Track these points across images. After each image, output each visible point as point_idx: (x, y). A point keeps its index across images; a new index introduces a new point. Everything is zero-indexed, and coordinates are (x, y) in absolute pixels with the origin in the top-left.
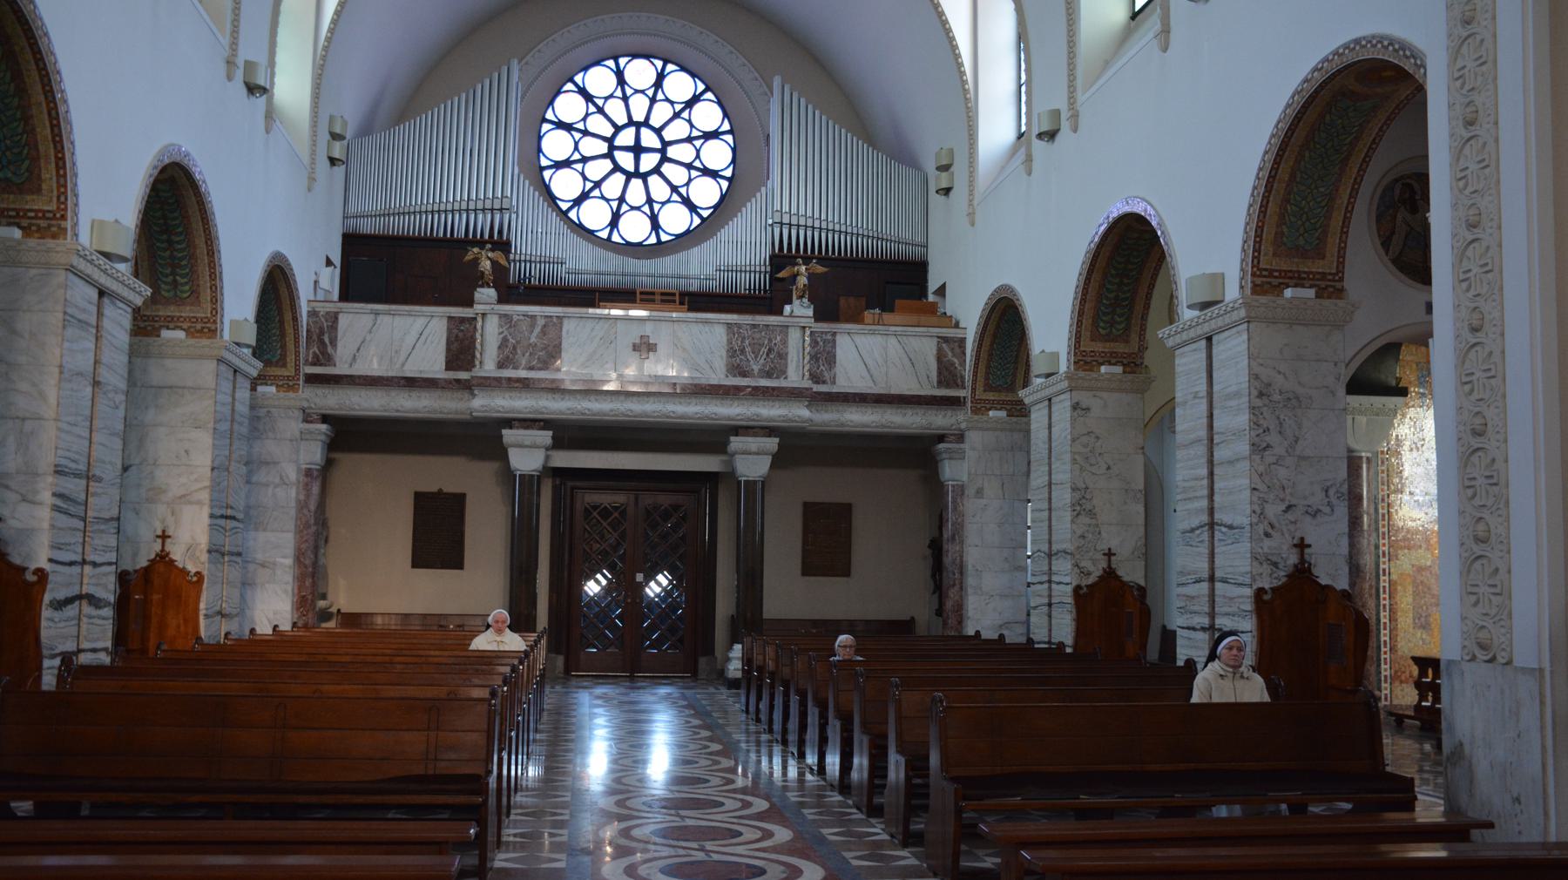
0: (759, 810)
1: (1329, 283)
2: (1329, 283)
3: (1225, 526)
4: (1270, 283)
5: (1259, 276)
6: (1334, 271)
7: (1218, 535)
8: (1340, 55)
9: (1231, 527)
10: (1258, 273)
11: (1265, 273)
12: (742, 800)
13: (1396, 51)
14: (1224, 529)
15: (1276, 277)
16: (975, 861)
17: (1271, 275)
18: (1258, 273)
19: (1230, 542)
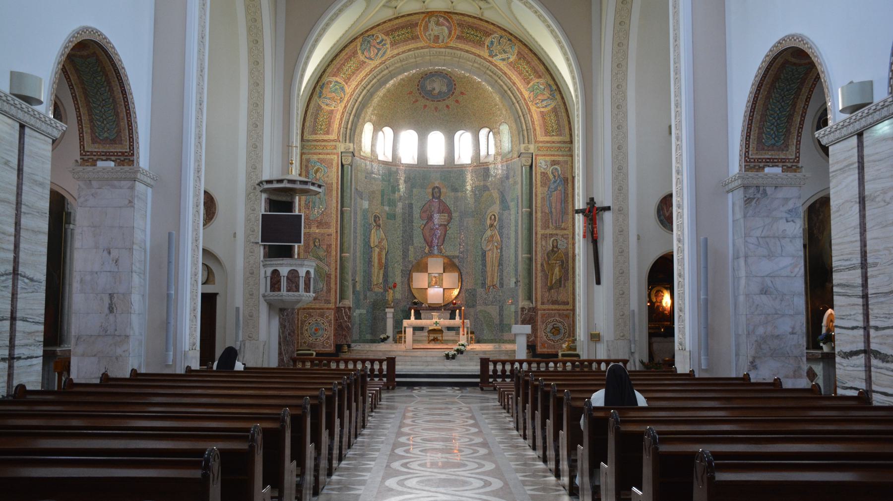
0: (401, 448)
1: (89, 157)
2: (89, 157)
3: (28, 278)
4: (92, 158)
5: (85, 155)
6: (86, 150)
7: (20, 284)
8: (76, 37)
9: (32, 280)
10: (84, 154)
11: (88, 153)
12: (473, 449)
13: (90, 32)
14: (26, 281)
15: (95, 155)
16: (534, 495)
17: (92, 154)
18: (84, 154)
19: (30, 290)
